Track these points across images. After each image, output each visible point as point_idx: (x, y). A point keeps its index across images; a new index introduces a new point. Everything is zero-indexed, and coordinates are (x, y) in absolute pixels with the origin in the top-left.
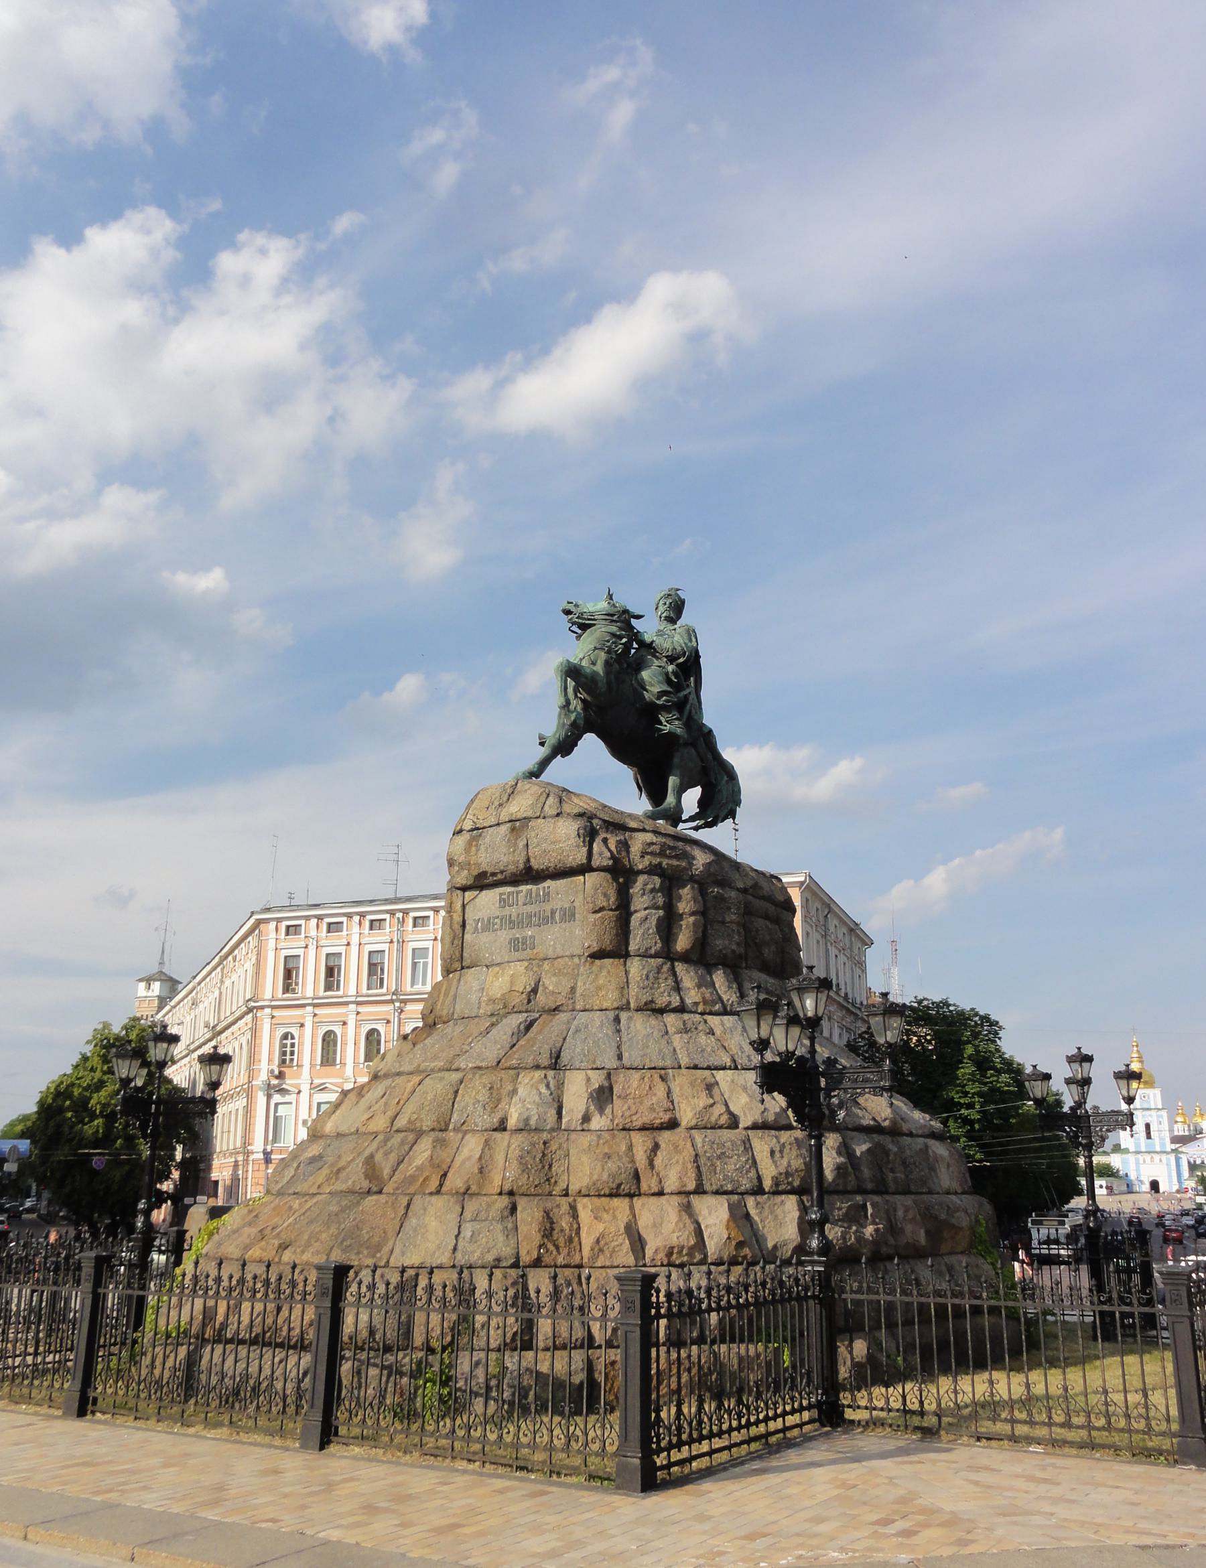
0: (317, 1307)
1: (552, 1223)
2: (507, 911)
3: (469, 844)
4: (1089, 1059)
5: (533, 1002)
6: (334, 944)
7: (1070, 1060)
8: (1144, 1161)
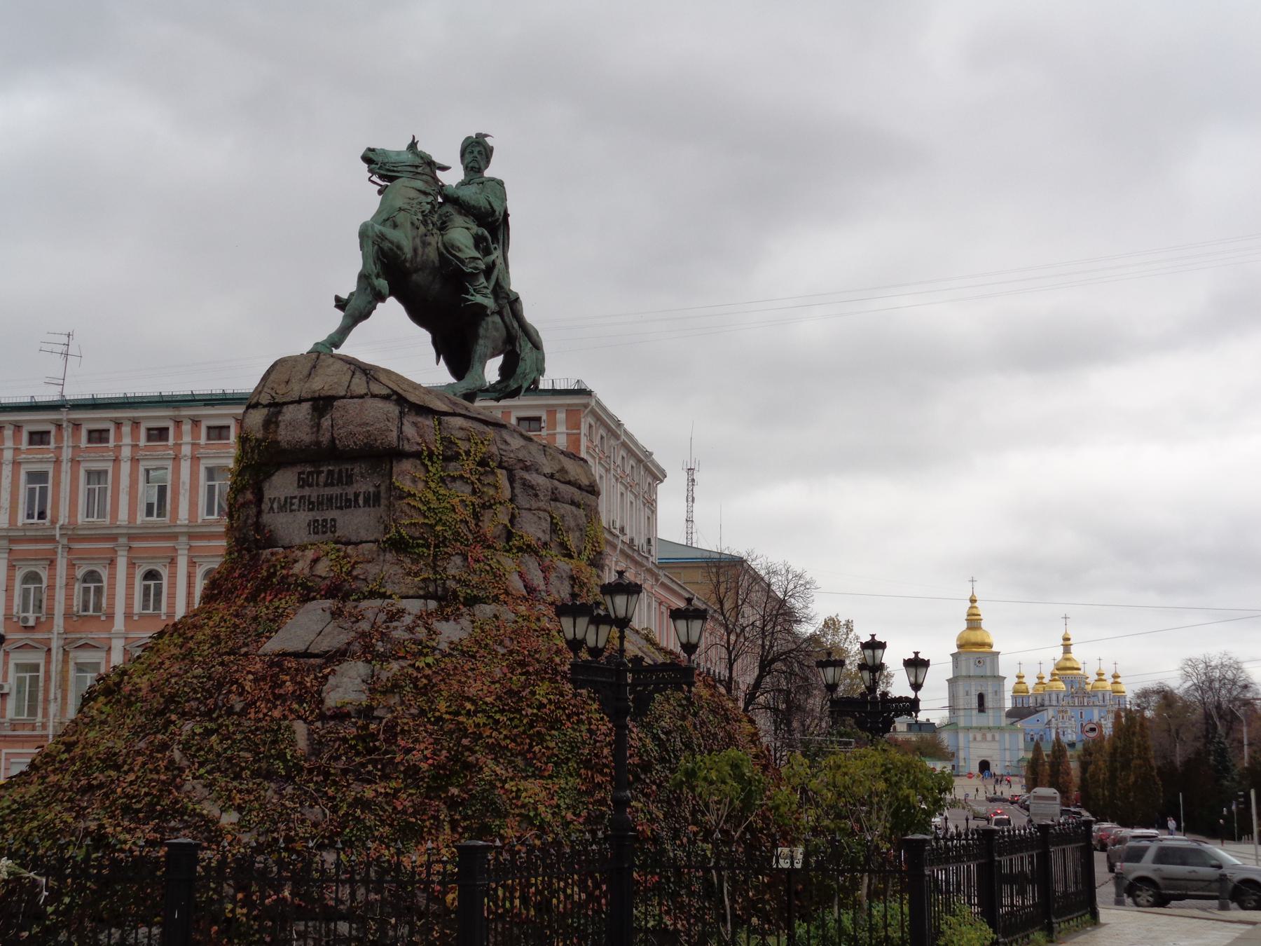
2: (307, 491)
7: (865, 646)
8: (975, 739)
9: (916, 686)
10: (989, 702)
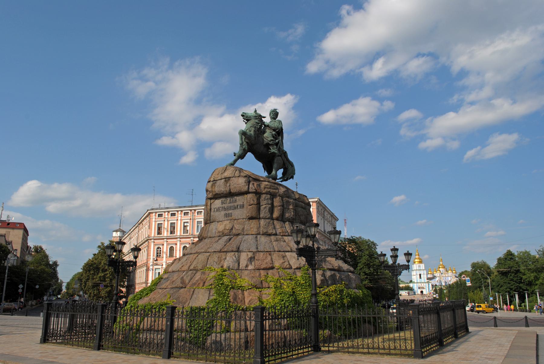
0: (166, 319)
1: (236, 296)
2: (224, 205)
3: (212, 185)
4: (397, 250)
5: (231, 232)
6: (173, 220)
7: (392, 250)
9: (408, 261)
10: (422, 276)
